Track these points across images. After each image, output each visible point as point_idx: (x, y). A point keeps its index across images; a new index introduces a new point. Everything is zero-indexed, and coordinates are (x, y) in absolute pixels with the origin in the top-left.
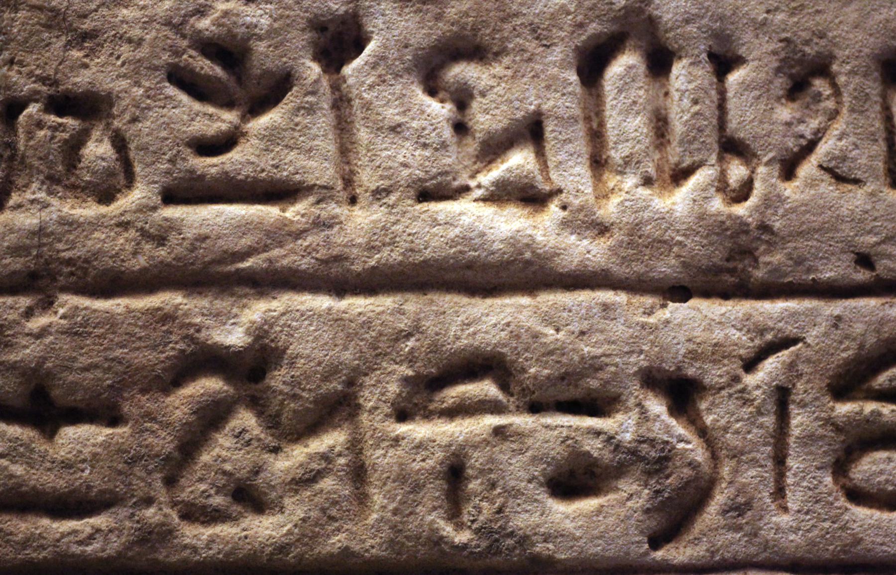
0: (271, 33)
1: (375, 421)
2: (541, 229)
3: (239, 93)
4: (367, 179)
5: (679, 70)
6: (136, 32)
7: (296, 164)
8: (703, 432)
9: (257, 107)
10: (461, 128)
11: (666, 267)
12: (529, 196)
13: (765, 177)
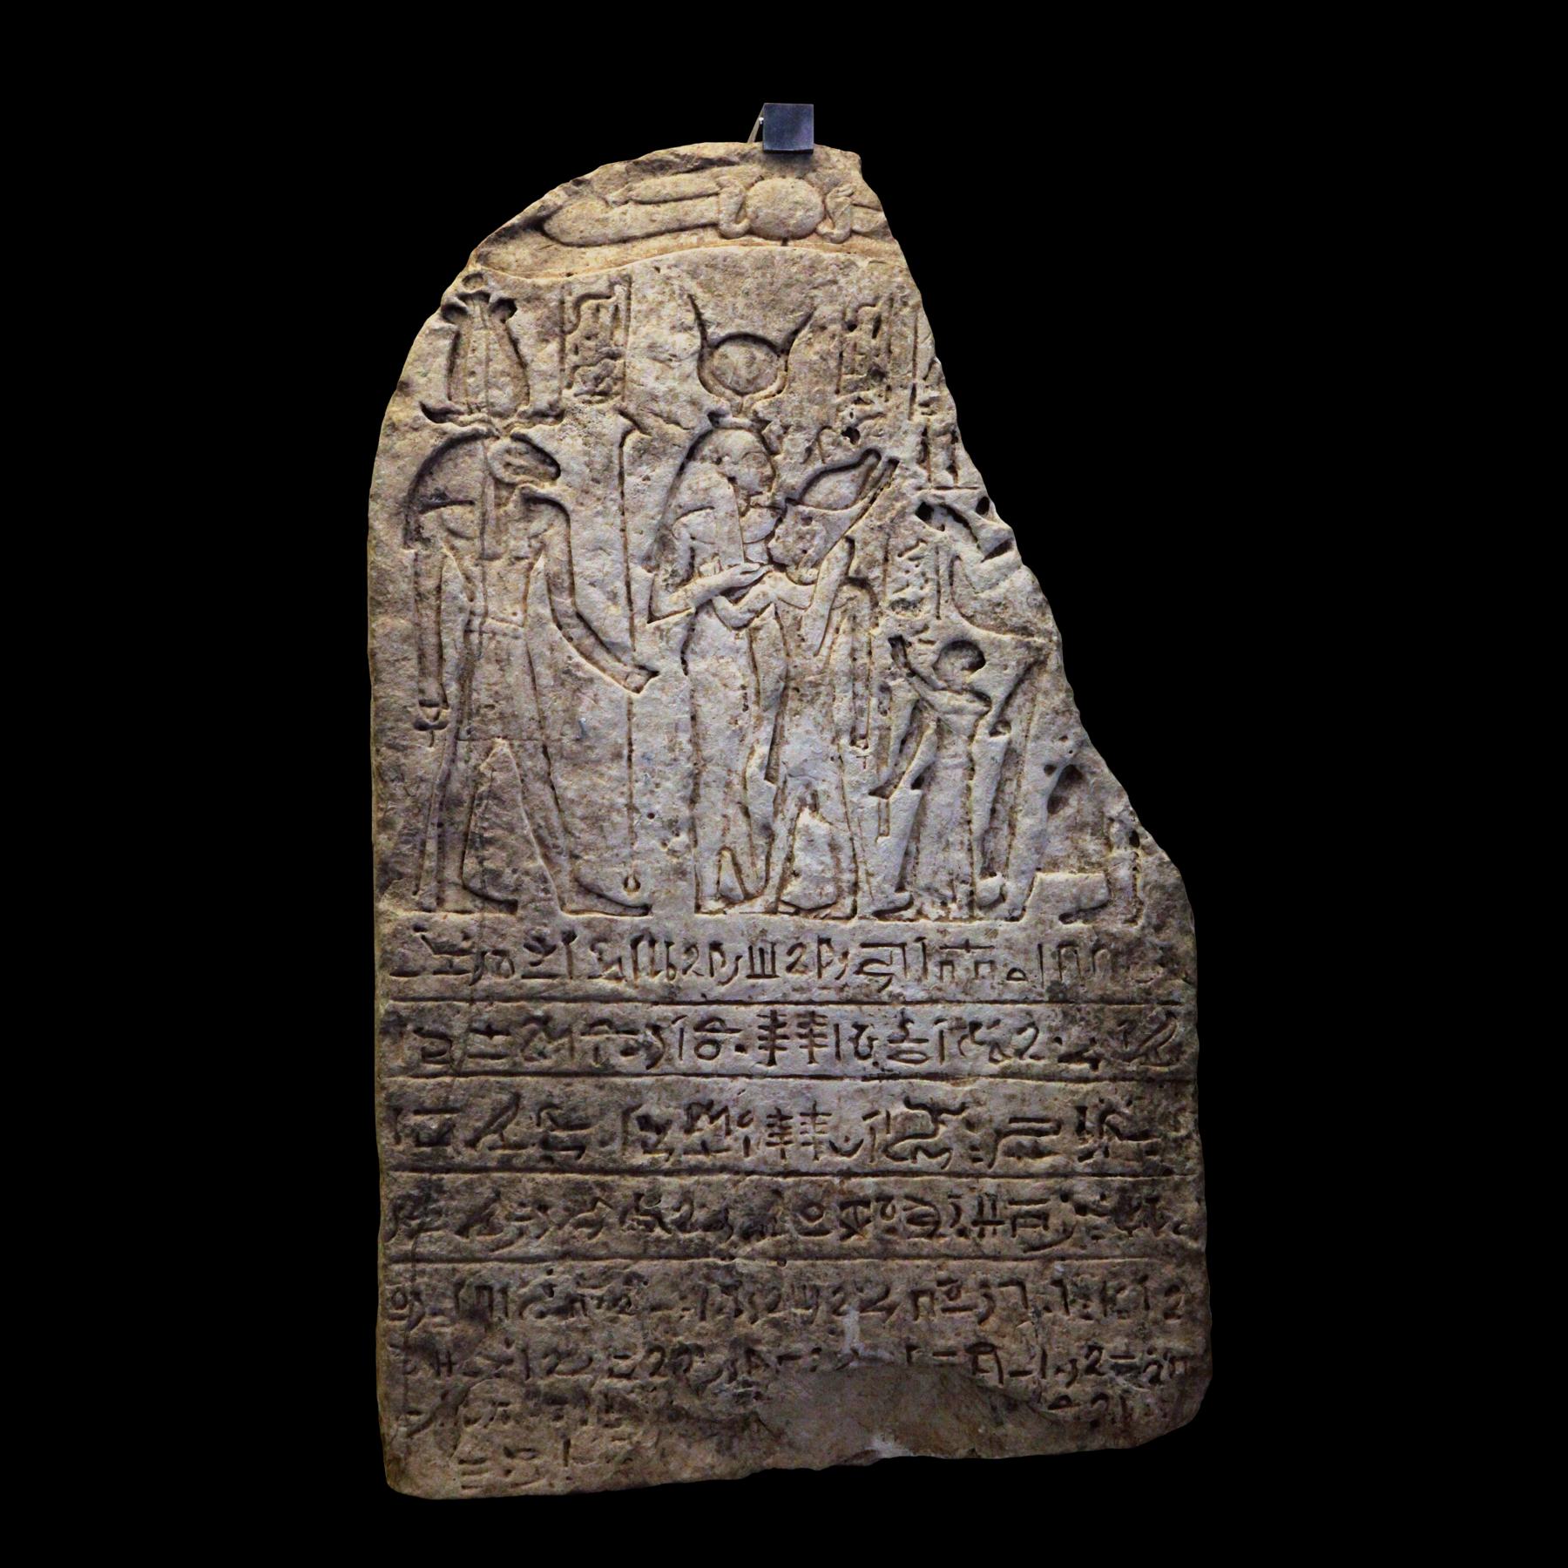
1: (576, 1035)
2: (621, 986)
4: (576, 973)
7: (555, 969)
8: (661, 1040)
9: (548, 953)
10: (600, 960)
11: (652, 997)
12: (618, 978)
13: (679, 973)
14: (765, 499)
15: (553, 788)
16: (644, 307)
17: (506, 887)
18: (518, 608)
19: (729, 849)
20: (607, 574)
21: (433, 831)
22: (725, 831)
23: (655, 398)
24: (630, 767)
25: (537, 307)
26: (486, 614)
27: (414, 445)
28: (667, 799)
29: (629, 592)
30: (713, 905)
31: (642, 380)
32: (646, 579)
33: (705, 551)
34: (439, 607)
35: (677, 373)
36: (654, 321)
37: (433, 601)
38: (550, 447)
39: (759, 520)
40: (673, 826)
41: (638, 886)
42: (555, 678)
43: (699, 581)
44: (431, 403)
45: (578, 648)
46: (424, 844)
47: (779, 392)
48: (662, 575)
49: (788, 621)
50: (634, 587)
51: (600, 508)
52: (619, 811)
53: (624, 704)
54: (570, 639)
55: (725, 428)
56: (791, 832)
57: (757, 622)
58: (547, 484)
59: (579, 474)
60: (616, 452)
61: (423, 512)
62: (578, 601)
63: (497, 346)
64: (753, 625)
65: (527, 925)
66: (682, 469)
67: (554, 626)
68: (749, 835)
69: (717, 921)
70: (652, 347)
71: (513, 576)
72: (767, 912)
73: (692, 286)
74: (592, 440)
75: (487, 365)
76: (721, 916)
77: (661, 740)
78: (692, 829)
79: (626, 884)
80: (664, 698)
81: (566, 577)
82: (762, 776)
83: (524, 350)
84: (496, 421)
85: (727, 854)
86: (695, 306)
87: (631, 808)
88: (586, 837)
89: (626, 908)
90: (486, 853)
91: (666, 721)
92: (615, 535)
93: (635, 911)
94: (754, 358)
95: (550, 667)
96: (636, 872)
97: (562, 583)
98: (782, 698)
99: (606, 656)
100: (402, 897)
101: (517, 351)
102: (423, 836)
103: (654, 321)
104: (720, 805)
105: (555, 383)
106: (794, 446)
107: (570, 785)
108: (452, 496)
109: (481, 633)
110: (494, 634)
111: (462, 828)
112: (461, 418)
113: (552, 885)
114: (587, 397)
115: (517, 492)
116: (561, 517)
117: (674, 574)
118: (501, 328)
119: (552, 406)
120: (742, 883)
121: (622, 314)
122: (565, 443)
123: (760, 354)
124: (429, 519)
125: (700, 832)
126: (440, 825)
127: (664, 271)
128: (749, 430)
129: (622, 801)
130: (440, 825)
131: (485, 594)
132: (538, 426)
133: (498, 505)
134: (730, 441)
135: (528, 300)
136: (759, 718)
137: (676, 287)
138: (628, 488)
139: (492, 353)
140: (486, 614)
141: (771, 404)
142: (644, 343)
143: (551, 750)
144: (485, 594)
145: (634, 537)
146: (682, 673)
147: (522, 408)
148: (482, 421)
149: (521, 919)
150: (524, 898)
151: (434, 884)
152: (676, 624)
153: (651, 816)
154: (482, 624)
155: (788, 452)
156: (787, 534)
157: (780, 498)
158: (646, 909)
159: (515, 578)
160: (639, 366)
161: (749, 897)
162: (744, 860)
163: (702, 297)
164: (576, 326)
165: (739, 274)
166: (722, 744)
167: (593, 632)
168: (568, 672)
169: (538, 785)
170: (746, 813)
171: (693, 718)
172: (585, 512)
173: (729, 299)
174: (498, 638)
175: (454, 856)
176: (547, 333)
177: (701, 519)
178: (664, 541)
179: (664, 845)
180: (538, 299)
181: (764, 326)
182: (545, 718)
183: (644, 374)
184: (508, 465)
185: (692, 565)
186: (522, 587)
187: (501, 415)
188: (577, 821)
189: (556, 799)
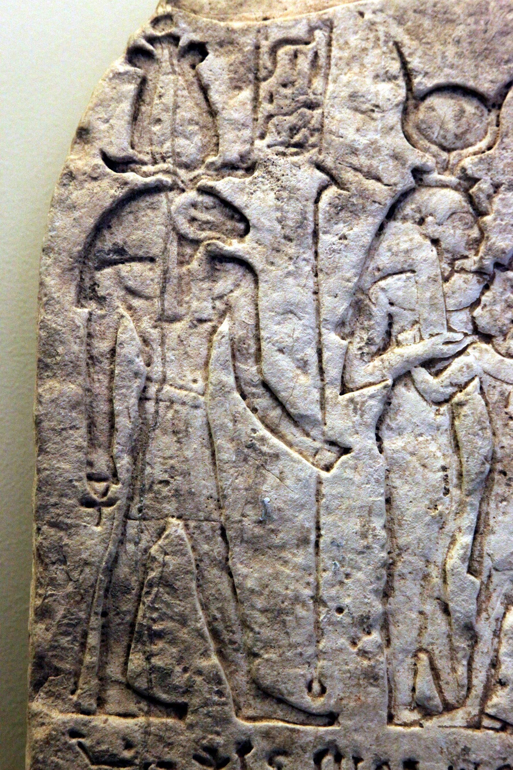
0: (224, 745)
3: (213, 762)
5: (344, 762)
6: (184, 744)
14: (471, 263)
15: (230, 575)
16: (346, 54)
17: (176, 688)
18: (199, 375)
19: (426, 651)
20: (298, 339)
21: (96, 622)
22: (422, 629)
23: (354, 152)
24: (317, 554)
25: (229, 52)
26: (164, 380)
27: (92, 195)
28: (357, 593)
29: (320, 361)
30: (407, 715)
31: (342, 131)
32: (340, 347)
33: (404, 318)
34: (112, 372)
35: (379, 125)
36: (356, 69)
37: (106, 365)
38: (239, 201)
39: (465, 286)
40: (365, 624)
41: (323, 690)
42: (238, 452)
43: (398, 350)
44: (113, 151)
45: (263, 420)
46: (85, 635)
47: (489, 148)
48: (357, 343)
49: (494, 397)
50: (326, 355)
51: (291, 268)
52: (304, 604)
53: (313, 482)
54: (255, 410)
55: (430, 186)
56: (497, 634)
57: (459, 397)
58: (235, 241)
59: (269, 231)
60: (311, 207)
61: (99, 269)
62: (265, 368)
63: (185, 93)
64: (455, 400)
65: (198, 732)
66: (381, 229)
67: (237, 395)
68: (449, 636)
69: (413, 735)
70: (353, 96)
71: (194, 341)
72: (468, 727)
73: (399, 33)
74: (285, 194)
75: (174, 112)
76: (416, 729)
77: (354, 525)
78: (385, 627)
79: (310, 688)
80: (357, 478)
81: (252, 342)
82: (464, 569)
83: (214, 96)
84: (182, 172)
85: (423, 656)
86: (401, 55)
87: (318, 600)
88: (267, 633)
89: (309, 716)
90: (154, 648)
91: (359, 503)
92: (308, 297)
93: (319, 721)
94: (463, 111)
95: (232, 440)
96: (322, 675)
97: (248, 348)
98: (487, 482)
99: (293, 429)
100: (58, 696)
101: (207, 100)
102: (84, 627)
103: (356, 69)
104: (416, 599)
105: (247, 133)
106: (505, 206)
107: (250, 572)
108: (131, 252)
109: (158, 401)
110: (172, 402)
111: (128, 618)
112: (145, 168)
113: (227, 686)
114: (281, 149)
115: (201, 249)
116: (249, 277)
117: (370, 342)
118: (190, 74)
119: (243, 157)
120: (441, 692)
121: (322, 61)
122: (255, 198)
123: (470, 107)
124: (105, 277)
125: (393, 629)
126: (104, 614)
127: (368, 16)
128: (456, 189)
129: (307, 592)
130: (104, 614)
131: (164, 358)
132: (227, 179)
133: (181, 263)
134: (434, 199)
135: (221, 44)
136: (462, 504)
137: (381, 34)
138: (322, 247)
139: (180, 99)
140: (164, 380)
141: (481, 159)
142: (345, 93)
143: (230, 533)
144: (164, 358)
145: (327, 301)
146: (376, 451)
147: (211, 159)
148: (167, 172)
149: (191, 727)
150: (196, 701)
151: (95, 682)
152: (372, 397)
153: (340, 610)
154: (159, 391)
155: (498, 212)
156: (494, 302)
157: (488, 262)
158: (331, 718)
159: (196, 341)
160: (338, 116)
161: (448, 708)
162: (442, 664)
163: (409, 44)
164: (271, 73)
165: (452, 21)
166: (420, 531)
167: (280, 404)
168: (251, 446)
169: (215, 571)
170: (446, 610)
171: (388, 501)
172: (275, 272)
173: (438, 47)
174: (176, 407)
175: (119, 650)
176: (239, 80)
177: (400, 283)
178: (359, 307)
179: (354, 643)
180: (231, 43)
181: (476, 77)
182: (225, 497)
183: (344, 125)
184: (193, 220)
185: (389, 334)
186: (204, 352)
187: (187, 167)
188: (257, 614)
189: (234, 588)
